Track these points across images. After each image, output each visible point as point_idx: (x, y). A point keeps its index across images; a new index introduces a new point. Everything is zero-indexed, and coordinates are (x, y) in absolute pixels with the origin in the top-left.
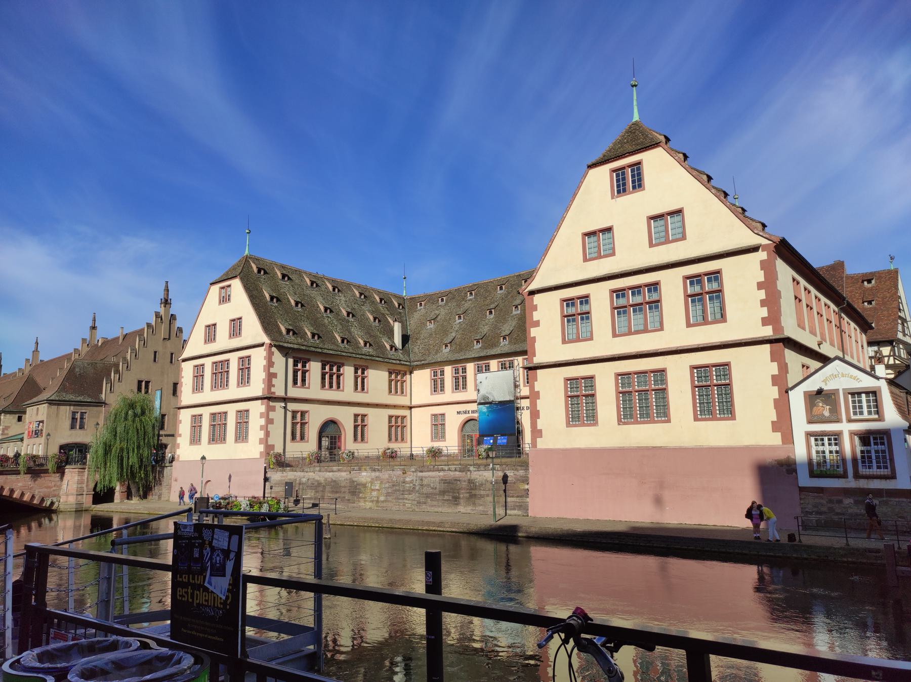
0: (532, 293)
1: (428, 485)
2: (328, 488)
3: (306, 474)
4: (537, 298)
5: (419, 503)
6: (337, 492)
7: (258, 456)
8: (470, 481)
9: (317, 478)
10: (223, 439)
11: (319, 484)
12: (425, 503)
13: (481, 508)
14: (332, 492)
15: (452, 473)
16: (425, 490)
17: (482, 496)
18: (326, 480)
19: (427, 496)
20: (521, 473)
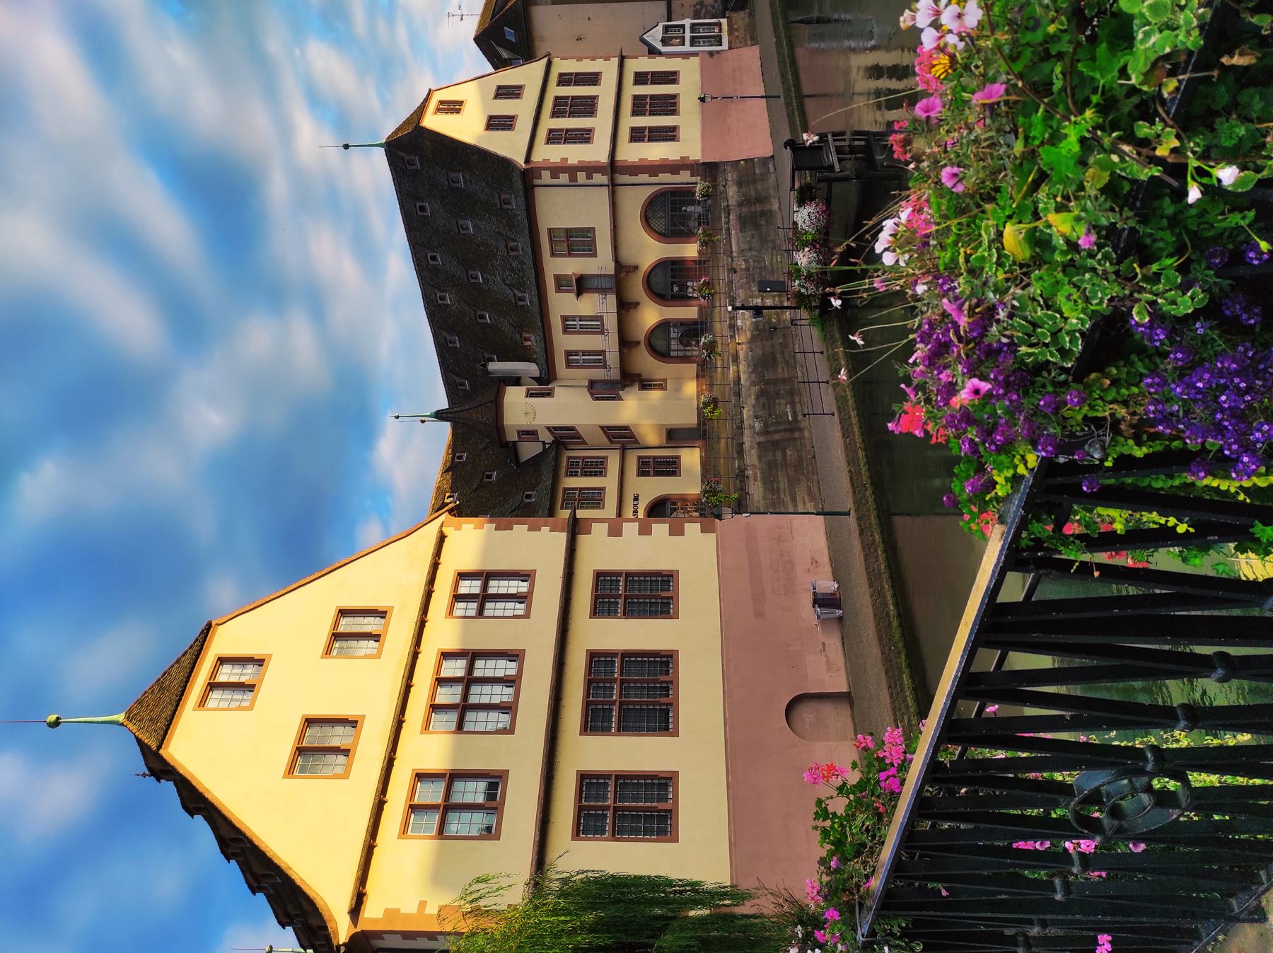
0: (528, 160)
1: (749, 242)
2: (769, 375)
3: (746, 424)
4: (537, 157)
5: (774, 248)
6: (774, 359)
7: (712, 537)
8: (740, 204)
9: (752, 400)
10: (662, 784)
11: (762, 394)
12: (774, 241)
13: (771, 191)
14: (775, 366)
15: (732, 222)
16: (756, 244)
17: (757, 191)
18: (753, 383)
19: (763, 241)
20: (728, 168)
